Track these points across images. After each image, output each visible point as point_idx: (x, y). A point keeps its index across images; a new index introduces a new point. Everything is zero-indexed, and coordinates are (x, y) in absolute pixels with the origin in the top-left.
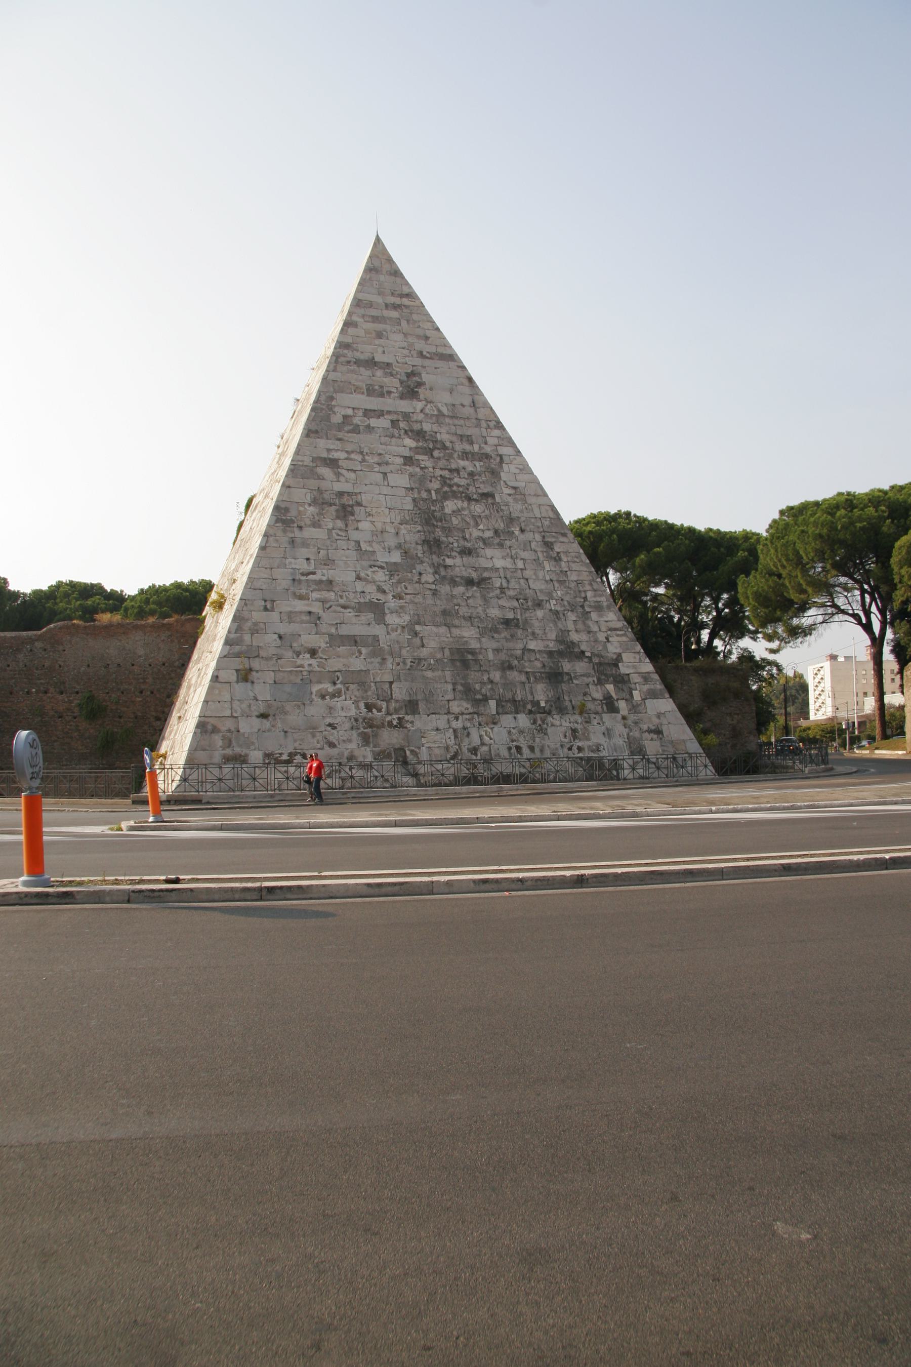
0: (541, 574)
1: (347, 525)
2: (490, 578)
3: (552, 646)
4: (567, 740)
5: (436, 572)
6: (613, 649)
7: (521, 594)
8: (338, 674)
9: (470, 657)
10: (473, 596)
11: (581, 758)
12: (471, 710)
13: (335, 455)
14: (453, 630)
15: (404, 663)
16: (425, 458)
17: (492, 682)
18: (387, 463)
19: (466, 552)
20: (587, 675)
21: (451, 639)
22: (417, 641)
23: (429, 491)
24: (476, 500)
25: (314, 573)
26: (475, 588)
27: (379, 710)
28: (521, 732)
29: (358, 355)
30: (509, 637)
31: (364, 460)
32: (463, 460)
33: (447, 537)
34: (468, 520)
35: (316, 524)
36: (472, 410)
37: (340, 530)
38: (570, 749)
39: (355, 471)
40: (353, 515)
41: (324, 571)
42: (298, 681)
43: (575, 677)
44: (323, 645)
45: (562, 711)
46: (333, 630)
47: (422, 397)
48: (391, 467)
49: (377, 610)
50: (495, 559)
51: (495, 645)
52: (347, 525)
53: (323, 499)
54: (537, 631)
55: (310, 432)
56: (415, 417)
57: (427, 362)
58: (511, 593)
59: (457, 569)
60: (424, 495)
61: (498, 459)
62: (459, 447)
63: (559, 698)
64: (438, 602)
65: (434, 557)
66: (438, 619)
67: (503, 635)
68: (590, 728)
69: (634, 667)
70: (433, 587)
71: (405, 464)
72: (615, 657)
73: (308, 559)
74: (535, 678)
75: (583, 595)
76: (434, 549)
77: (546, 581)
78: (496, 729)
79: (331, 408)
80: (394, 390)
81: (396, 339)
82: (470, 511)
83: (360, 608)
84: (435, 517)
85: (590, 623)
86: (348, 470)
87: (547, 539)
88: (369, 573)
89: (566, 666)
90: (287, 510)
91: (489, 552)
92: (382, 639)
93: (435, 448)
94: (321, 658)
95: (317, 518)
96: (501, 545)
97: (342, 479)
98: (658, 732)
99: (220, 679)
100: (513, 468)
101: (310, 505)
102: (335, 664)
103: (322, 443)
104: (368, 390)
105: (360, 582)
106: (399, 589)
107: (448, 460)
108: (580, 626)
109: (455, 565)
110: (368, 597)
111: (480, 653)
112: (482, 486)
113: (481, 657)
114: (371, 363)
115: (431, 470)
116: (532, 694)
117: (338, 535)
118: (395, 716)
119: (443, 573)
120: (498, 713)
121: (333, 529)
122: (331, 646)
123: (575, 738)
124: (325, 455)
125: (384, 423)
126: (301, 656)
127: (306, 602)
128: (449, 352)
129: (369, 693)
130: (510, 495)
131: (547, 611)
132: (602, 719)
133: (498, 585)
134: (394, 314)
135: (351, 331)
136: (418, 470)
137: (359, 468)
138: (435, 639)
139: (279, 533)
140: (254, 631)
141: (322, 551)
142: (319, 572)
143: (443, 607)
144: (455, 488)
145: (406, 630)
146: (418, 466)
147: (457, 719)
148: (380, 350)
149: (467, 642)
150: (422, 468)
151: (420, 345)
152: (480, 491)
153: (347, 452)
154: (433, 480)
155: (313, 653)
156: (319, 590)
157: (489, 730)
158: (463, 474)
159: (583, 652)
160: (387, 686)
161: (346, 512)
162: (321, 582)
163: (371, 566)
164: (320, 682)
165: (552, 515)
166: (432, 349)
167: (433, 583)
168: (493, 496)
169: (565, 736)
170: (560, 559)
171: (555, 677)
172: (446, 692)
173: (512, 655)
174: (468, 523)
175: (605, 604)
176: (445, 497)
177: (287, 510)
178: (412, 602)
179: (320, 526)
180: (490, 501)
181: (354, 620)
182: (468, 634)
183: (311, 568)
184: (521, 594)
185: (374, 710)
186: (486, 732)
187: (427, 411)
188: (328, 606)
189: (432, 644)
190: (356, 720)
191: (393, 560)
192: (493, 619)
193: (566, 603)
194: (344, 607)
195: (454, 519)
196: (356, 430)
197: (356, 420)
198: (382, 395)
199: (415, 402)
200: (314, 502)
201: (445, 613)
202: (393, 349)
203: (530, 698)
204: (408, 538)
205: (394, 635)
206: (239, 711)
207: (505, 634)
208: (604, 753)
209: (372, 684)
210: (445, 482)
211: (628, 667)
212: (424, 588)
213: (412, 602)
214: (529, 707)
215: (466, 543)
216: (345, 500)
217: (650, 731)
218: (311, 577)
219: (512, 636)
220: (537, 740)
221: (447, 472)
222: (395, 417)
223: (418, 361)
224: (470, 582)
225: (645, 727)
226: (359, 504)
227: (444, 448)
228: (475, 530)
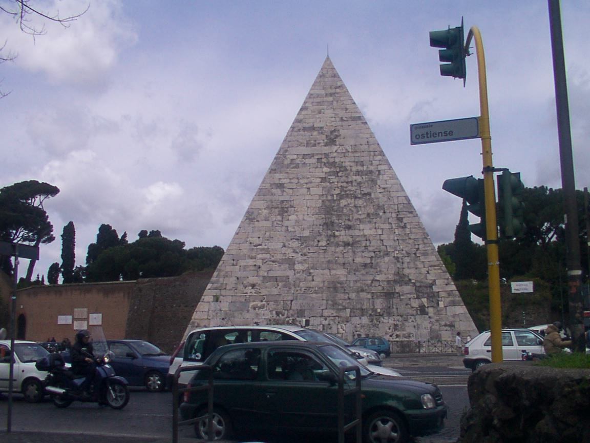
0: (392, 236)
1: (282, 218)
3: (391, 277)
4: (390, 331)
5: (328, 240)
6: (430, 277)
7: (377, 249)
8: (265, 296)
9: (339, 285)
11: (397, 342)
12: (334, 315)
13: (283, 181)
14: (332, 271)
15: (301, 290)
17: (349, 299)
19: (349, 227)
20: (410, 294)
21: (330, 276)
22: (310, 278)
24: (359, 198)
25: (261, 245)
26: (350, 247)
27: (283, 315)
28: (362, 326)
29: (307, 126)
30: (365, 273)
32: (356, 175)
33: (338, 220)
34: (352, 209)
35: (266, 219)
36: (366, 147)
38: (391, 336)
41: (266, 244)
42: (243, 300)
43: (402, 295)
44: (259, 282)
45: (390, 314)
46: (266, 274)
47: (337, 143)
48: (312, 185)
49: (291, 263)
50: (367, 230)
51: (355, 279)
54: (382, 269)
55: (272, 171)
56: (331, 155)
57: (344, 123)
58: (370, 249)
59: (341, 237)
61: (378, 172)
62: (354, 169)
63: (389, 307)
67: (361, 272)
68: (407, 324)
69: (441, 288)
70: (325, 248)
72: (431, 282)
73: (259, 238)
74: (377, 296)
75: (417, 247)
76: (330, 227)
77: (394, 240)
78: (348, 324)
79: (285, 156)
80: (322, 141)
81: (329, 113)
83: (281, 263)
84: (333, 209)
85: (418, 263)
87: (399, 216)
88: (290, 243)
89: (398, 289)
90: (252, 213)
91: (362, 227)
93: (340, 171)
94: (257, 289)
96: (370, 222)
97: (285, 193)
98: (452, 326)
99: (205, 300)
100: (385, 177)
101: (265, 209)
102: (264, 292)
103: (277, 176)
104: (307, 143)
105: (284, 248)
108: (412, 265)
110: (287, 256)
113: (346, 285)
114: (313, 128)
115: (336, 183)
116: (373, 305)
117: (277, 224)
118: (291, 318)
120: (350, 316)
121: (275, 221)
123: (395, 329)
124: (277, 182)
125: (314, 160)
126: (247, 288)
127: (254, 260)
128: (358, 115)
129: (279, 306)
130: (380, 193)
131: (392, 257)
132: (415, 319)
133: (364, 245)
134: (331, 99)
135: (304, 112)
136: (328, 184)
138: (321, 276)
139: (246, 225)
140: (225, 276)
142: (263, 244)
144: (348, 192)
145: (305, 272)
146: (329, 182)
147: (326, 320)
148: (318, 120)
149: (339, 277)
150: (331, 183)
151: (342, 113)
152: (363, 192)
153: (290, 179)
155: (253, 286)
157: (344, 325)
158: (355, 184)
159: (410, 280)
160: (290, 302)
162: (264, 249)
163: (292, 239)
164: (254, 301)
165: (405, 202)
166: (349, 115)
167: (325, 246)
168: (369, 194)
169: (389, 329)
170: (406, 227)
171: (389, 295)
172: (322, 305)
173: (365, 284)
174: (353, 211)
175: (430, 252)
176: (341, 197)
177: (252, 213)
179: (268, 220)
180: (368, 197)
182: (340, 273)
183: (260, 243)
184: (377, 249)
185: (280, 315)
186: (341, 326)
187: (339, 151)
188: (265, 261)
189: (318, 279)
190: (270, 320)
193: (404, 252)
194: (273, 262)
195: (344, 209)
196: (297, 166)
197: (298, 161)
198: (315, 145)
199: (333, 147)
200: (268, 207)
202: (326, 120)
203: (372, 307)
205: (298, 275)
206: (211, 316)
207: (363, 272)
208: (412, 339)
209: (282, 302)
211: (438, 288)
214: (370, 312)
216: (285, 205)
217: (446, 325)
218: (258, 247)
219: (367, 273)
220: (372, 331)
221: (345, 183)
222: (320, 156)
223: (340, 123)
224: (347, 244)
225: (443, 323)
227: (346, 170)
228: (356, 215)
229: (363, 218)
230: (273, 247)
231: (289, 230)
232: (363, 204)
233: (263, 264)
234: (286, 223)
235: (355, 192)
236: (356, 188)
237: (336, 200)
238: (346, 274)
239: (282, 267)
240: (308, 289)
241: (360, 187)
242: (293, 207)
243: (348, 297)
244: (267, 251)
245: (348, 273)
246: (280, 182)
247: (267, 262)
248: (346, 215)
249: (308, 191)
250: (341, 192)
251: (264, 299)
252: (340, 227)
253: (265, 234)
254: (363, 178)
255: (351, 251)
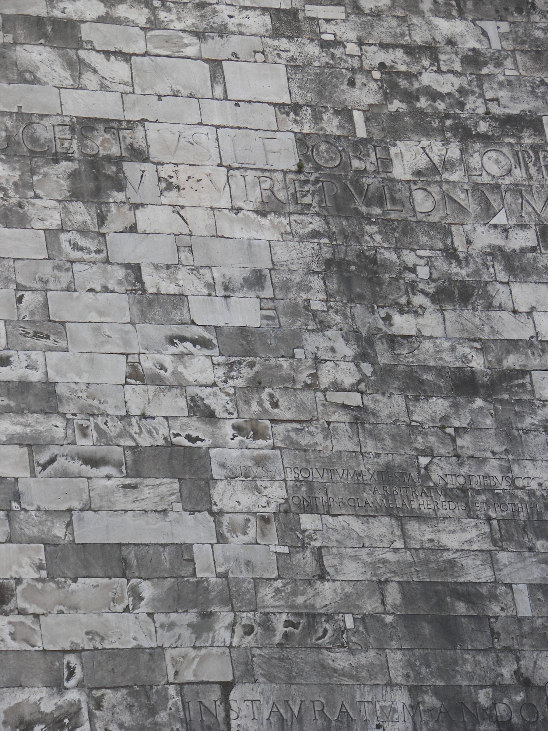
2: (524, 372)
5: (363, 356)
8: (72, 659)
9: (461, 608)
10: (473, 428)
14: (413, 527)
15: (267, 627)
16: (337, 12)
18: (223, 32)
19: (454, 294)
21: (408, 556)
23: (345, 113)
24: (485, 138)
26: (479, 403)
31: (154, 24)
32: (448, 16)
33: (397, 250)
34: (460, 197)
37: (84, 232)
39: (127, 57)
40: (121, 188)
46: (59, 531)
48: (234, 43)
49: (186, 468)
51: (537, 573)
52: (102, 219)
53: (35, 140)
59: (427, 345)
60: (332, 125)
64: (370, 446)
65: (358, 309)
66: (367, 496)
71: (276, 34)
82: (468, 170)
83: (139, 464)
84: (361, 191)
86: (107, 54)
88: (167, 361)
92: (202, 555)
94: (22, 612)
95: (14, 198)
97: (89, 79)
102: (61, 631)
105: (140, 388)
106: (255, 407)
107: (403, 19)
109: (420, 336)
110: (163, 431)
111: (493, 597)
112: (504, 94)
113: (495, 609)
115: (352, 48)
117: (76, 247)
119: (384, 359)
121: (62, 229)
122: (51, 577)
129: (163, 717)
136: (313, 49)
137: (139, 47)
138: (360, 549)
141: (28, 296)
142: (19, 358)
143: (383, 460)
144: (423, 103)
145: (273, 526)
146: (315, 36)
149: (452, 563)
150: (325, 45)
152: (495, 109)
154: (360, 79)
156: (20, 412)
160: (216, 694)
161: (98, 181)
162: (24, 386)
163: (171, 341)
174: (462, 209)
176: (395, 129)
178: (292, 445)
179: (23, 222)
181: (122, 501)
182: (459, 537)
188: (44, 458)
191: (238, 321)
192: (531, 493)
194: (93, 462)
195: (419, 196)
201: (388, 476)
204: (282, 253)
209: (172, 690)
210: (394, 86)
212: (327, 404)
213: (292, 445)
215: (455, 269)
216: (103, 144)
221: (399, 54)
224: (464, 384)
226: (139, 155)
228: (480, 229)
229: (523, 250)
230: (72, 377)
231: (151, 290)
232: (509, 172)
233: (33, 474)
234: (125, 248)
235: (462, 105)
236: (457, 82)
237: (364, 142)
238: (487, 546)
239: (146, 492)
240: (303, 621)
241: (480, 78)
242: (146, 160)
243: (517, 673)
244: (44, 397)
245: (494, 542)
246: (57, 13)
247: (52, 461)
248: (432, 225)
249: (213, 79)
250: (387, 98)
251: (71, 673)
252: (413, 287)
253: (20, 300)
254: (484, 33)
255: (489, 421)
